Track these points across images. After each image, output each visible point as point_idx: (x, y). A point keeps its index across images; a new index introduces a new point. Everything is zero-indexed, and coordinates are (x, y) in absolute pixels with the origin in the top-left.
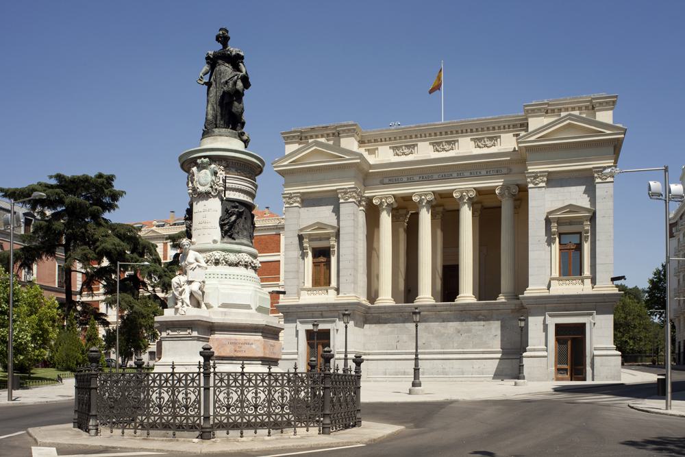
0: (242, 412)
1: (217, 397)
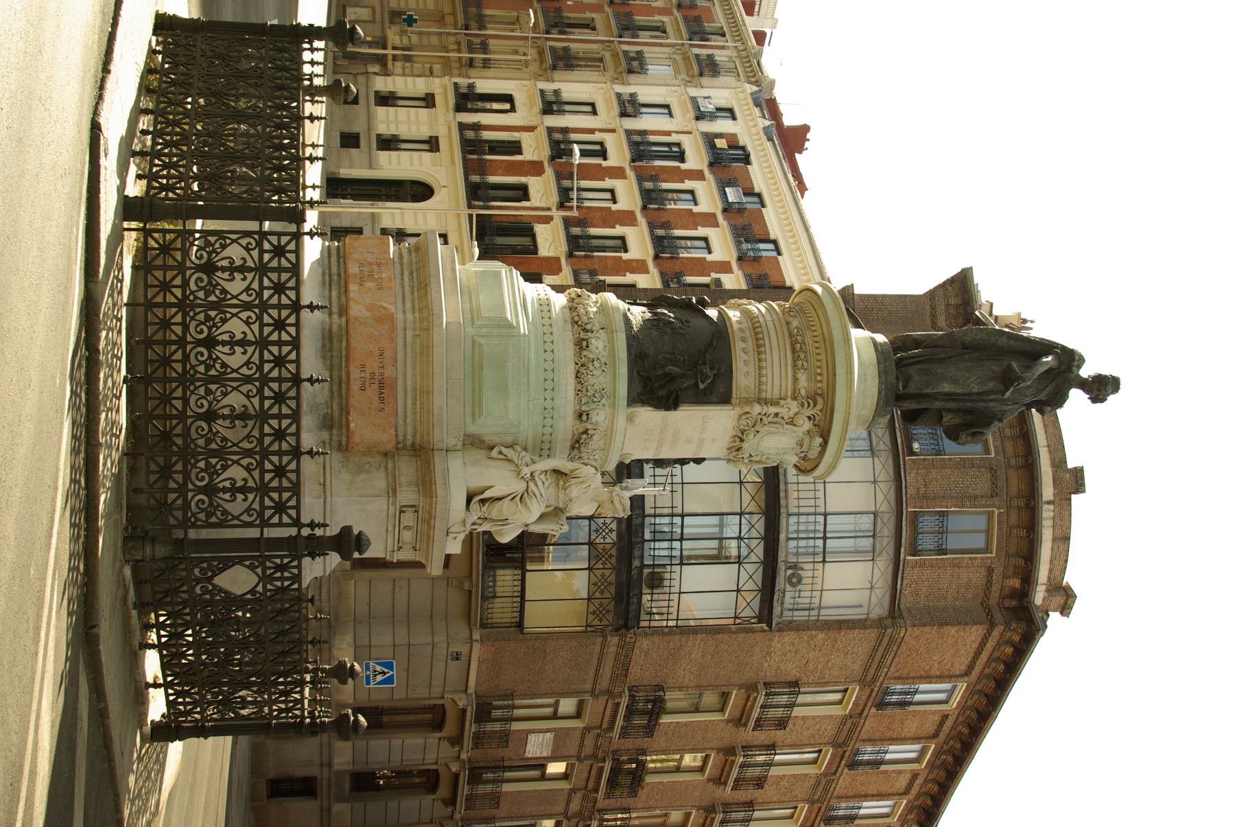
0: (193, 306)
1: (233, 241)
